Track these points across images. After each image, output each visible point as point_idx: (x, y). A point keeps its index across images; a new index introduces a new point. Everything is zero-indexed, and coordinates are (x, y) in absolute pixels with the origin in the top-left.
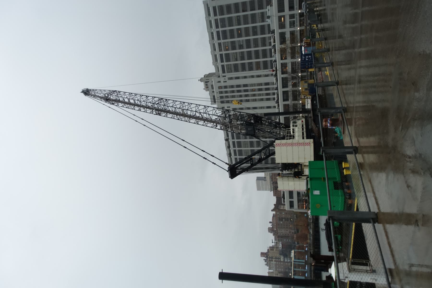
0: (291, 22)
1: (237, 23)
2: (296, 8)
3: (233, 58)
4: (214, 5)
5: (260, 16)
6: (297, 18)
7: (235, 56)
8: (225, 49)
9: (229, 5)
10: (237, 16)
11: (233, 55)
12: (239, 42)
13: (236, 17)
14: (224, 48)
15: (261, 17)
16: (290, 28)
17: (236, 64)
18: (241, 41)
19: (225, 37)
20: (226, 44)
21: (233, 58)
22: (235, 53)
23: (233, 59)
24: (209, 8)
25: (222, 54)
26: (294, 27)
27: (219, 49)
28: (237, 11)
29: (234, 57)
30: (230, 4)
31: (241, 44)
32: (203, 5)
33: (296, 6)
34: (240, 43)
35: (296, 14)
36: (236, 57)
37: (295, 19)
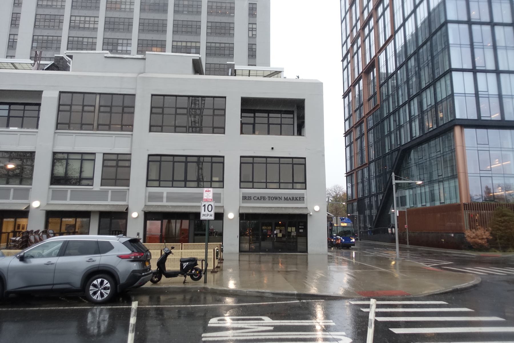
0: (87, 166)
1: (179, 44)
2: (159, 197)
3: (83, 19)
6: (102, 195)
7: (87, 26)
9: (231, 32)
11: (92, 19)
12: (125, 42)
13: (198, 45)
16: (54, 153)
17: (61, 22)
21: (83, 19)
22: (96, 26)
23: (78, 18)
26: (55, 180)
29: (85, 21)
31: (120, 48)
33: (170, 198)
34: (122, 45)
35: (123, 196)
36: (82, 25)
37: (97, 186)
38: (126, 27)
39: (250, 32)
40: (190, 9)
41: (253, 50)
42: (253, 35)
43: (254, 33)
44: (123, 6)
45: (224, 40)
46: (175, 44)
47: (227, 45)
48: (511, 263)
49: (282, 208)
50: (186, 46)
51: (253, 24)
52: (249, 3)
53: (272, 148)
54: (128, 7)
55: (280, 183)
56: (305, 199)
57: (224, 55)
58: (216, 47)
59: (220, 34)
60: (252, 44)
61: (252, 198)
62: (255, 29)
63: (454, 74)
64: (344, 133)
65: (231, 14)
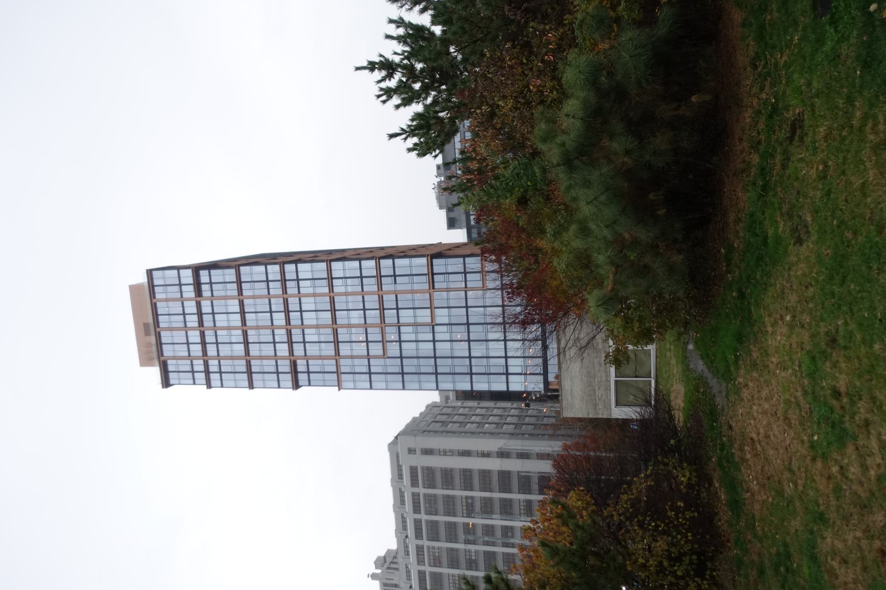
1: (465, 511)
3: (451, 585)
4: (414, 464)
5: (522, 507)
8: (432, 561)
10: (467, 498)
11: (451, 578)
12: (467, 553)
14: (430, 559)
15: (524, 510)
18: (473, 551)
19: (434, 536)
20: (437, 551)
25: (425, 571)
27: (418, 558)
28: (468, 486)
30: (452, 470)
31: (473, 558)
38: (455, 553)
39: (448, 454)
40: (433, 502)
44: (437, 554)
46: (465, 515)
50: (466, 506)
54: (437, 551)
58: (464, 483)
59: (452, 478)
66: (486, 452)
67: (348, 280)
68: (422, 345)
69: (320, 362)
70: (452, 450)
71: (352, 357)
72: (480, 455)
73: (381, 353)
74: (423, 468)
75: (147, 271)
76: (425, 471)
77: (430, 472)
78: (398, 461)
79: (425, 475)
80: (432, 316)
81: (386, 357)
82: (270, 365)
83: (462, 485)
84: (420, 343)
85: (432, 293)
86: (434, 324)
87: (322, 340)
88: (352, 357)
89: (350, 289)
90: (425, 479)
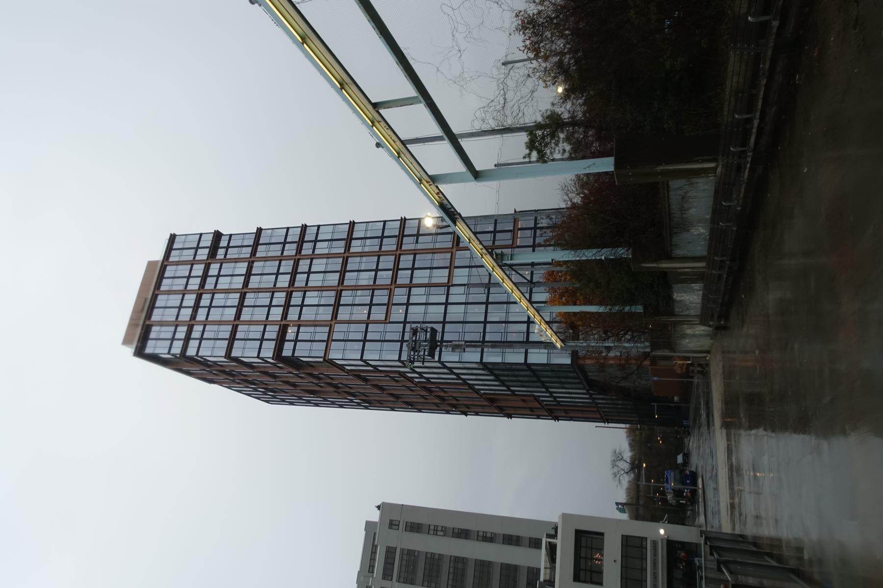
24: (376, 547)
30: (441, 556)
32: (362, 534)
39: (439, 533)
41: (460, 532)
42: (442, 531)
43: (440, 528)
45: (445, 567)
47: (451, 565)
48: (697, 419)
49: (662, 560)
51: (429, 529)
52: (405, 531)
53: (615, 561)
55: (642, 559)
56: (654, 539)
57: (463, 570)
58: (453, 579)
60: (453, 533)
61: (655, 583)
62: (436, 527)
63: (529, 362)
64: (553, 421)
65: (416, 554)
66: (489, 535)
67: (368, 241)
68: (431, 308)
69: (311, 329)
70: (446, 528)
71: (349, 322)
72: (480, 538)
73: (383, 317)
74: (402, 550)
75: (171, 235)
76: (405, 557)
77: (411, 556)
78: (374, 539)
79: (404, 563)
80: (450, 276)
81: (388, 321)
82: (256, 331)
83: (450, 582)
84: (430, 306)
85: (454, 253)
86: (450, 284)
87: (322, 303)
88: (349, 322)
89: (367, 249)
90: (403, 569)
